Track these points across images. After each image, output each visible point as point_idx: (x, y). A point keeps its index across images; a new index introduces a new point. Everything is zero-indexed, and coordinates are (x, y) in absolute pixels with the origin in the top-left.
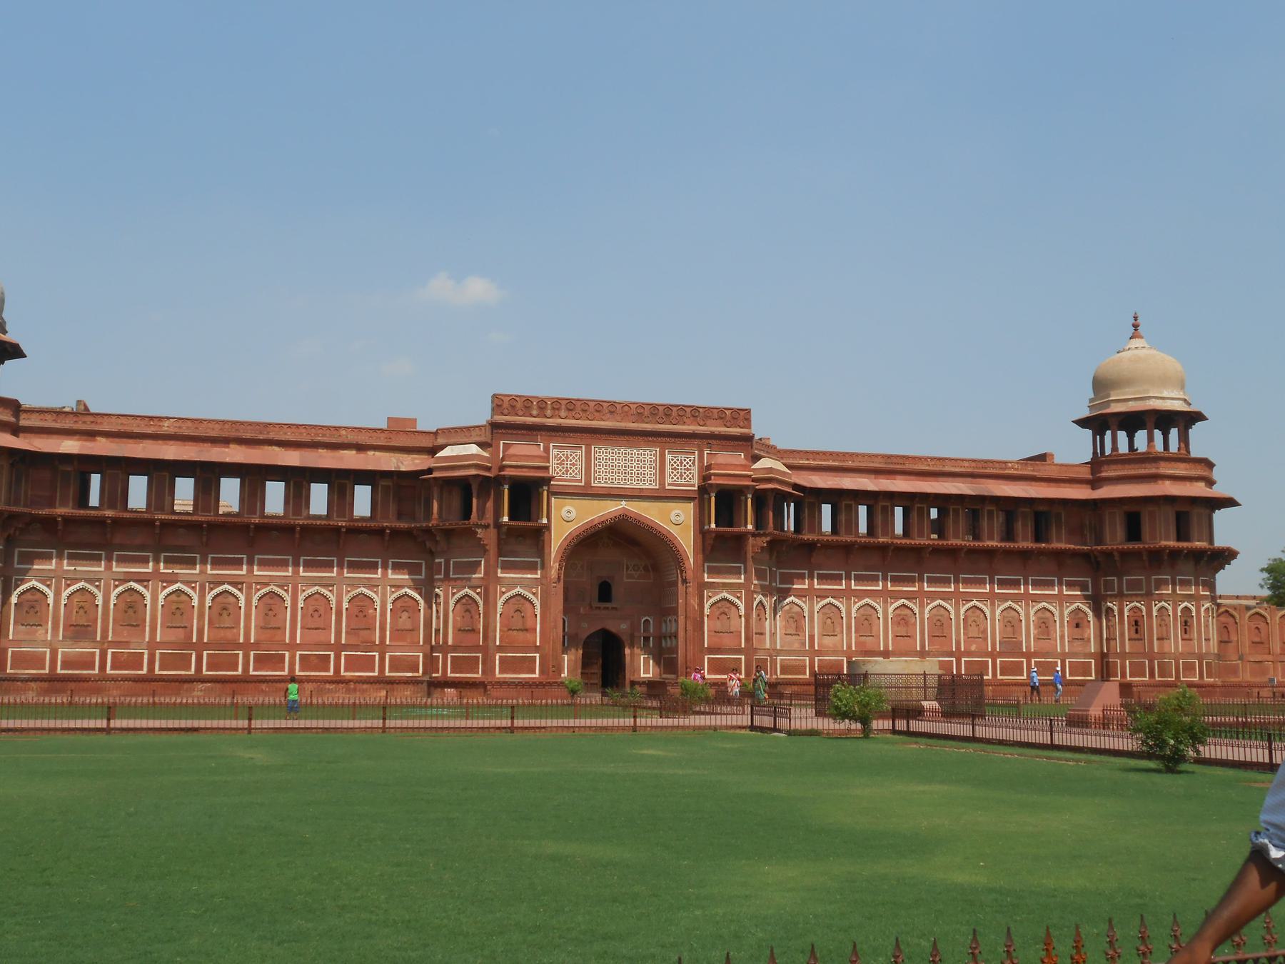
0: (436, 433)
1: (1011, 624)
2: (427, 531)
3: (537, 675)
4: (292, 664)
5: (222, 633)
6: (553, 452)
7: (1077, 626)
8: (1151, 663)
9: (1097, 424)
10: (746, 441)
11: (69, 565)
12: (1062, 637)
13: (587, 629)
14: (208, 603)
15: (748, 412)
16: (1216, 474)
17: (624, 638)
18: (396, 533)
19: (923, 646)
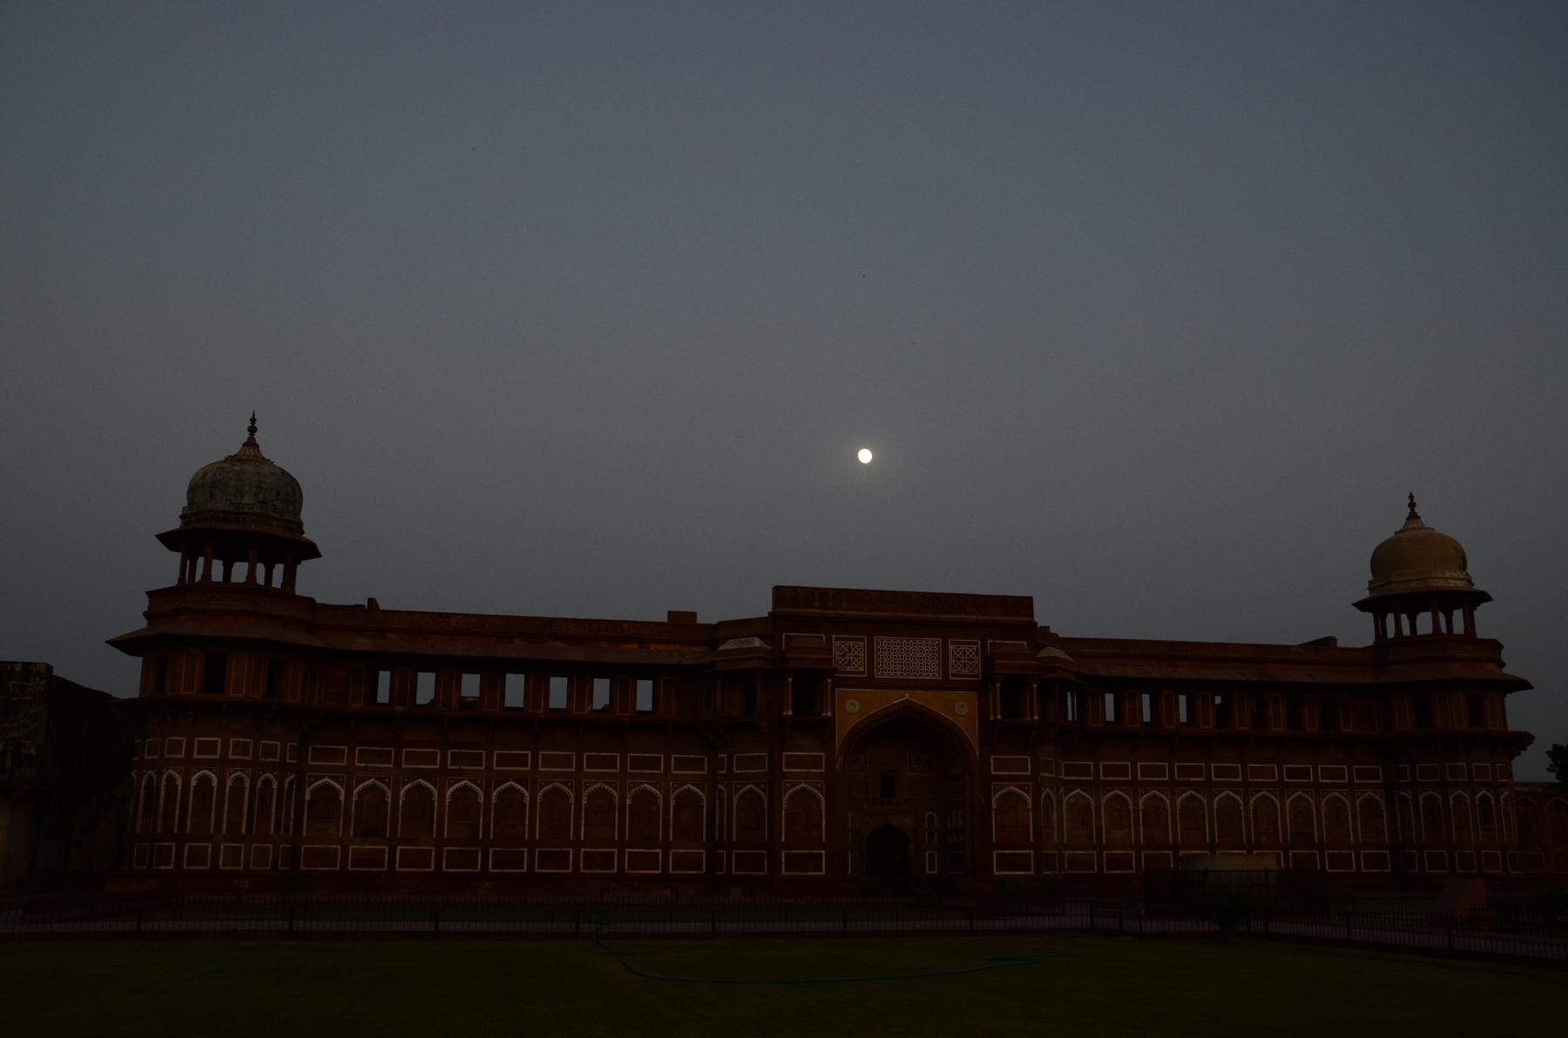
12: (1355, 828)
14: (494, 800)
15: (1031, 599)
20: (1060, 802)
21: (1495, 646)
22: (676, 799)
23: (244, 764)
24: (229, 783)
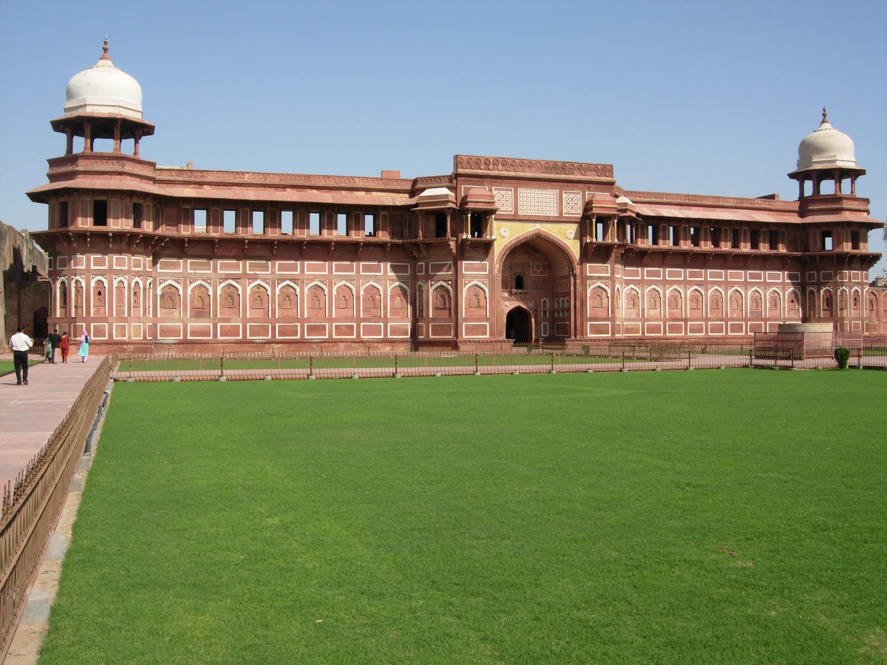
0: (415, 182)
1: (757, 301)
2: (417, 245)
3: (488, 336)
4: (330, 331)
5: (286, 312)
6: (495, 193)
9: (800, 176)
10: (609, 185)
11: (191, 269)
15: (612, 167)
16: (870, 207)
19: (707, 315)
21: (867, 201)
23: (123, 273)
24: (115, 284)
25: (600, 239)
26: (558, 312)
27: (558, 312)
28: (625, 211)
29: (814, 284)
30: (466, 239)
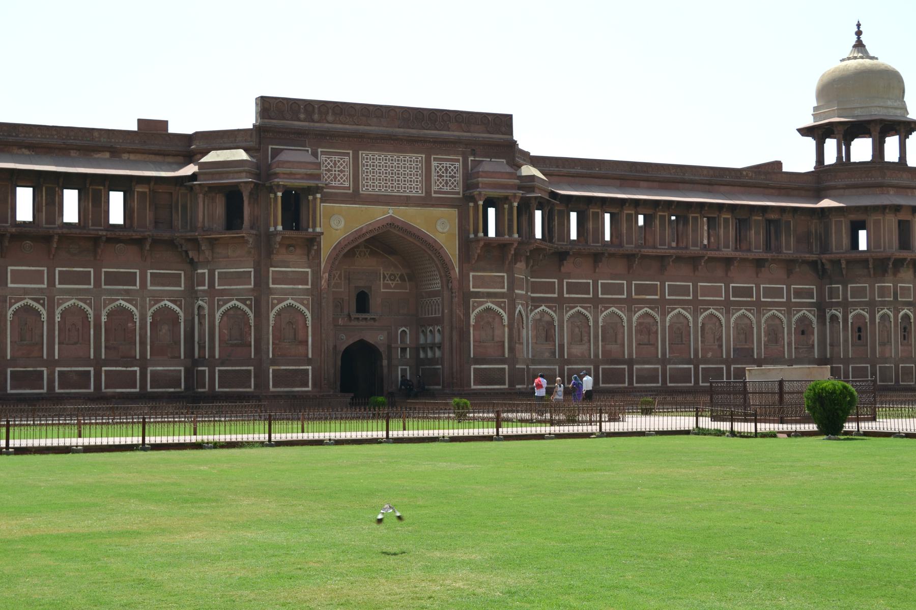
1: (744, 331)
2: (195, 242)
3: (310, 389)
4: (50, 379)
7: (803, 333)
8: (873, 367)
12: (789, 344)
13: (346, 340)
15: (509, 118)
17: (382, 349)
18: (156, 242)
19: (664, 354)
20: (527, 317)
22: (153, 316)
25: (492, 233)
26: (424, 349)
27: (424, 349)
28: (532, 189)
29: (838, 304)
30: (276, 233)
